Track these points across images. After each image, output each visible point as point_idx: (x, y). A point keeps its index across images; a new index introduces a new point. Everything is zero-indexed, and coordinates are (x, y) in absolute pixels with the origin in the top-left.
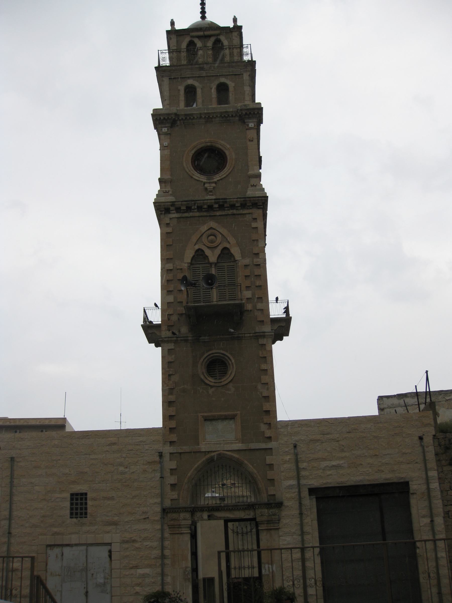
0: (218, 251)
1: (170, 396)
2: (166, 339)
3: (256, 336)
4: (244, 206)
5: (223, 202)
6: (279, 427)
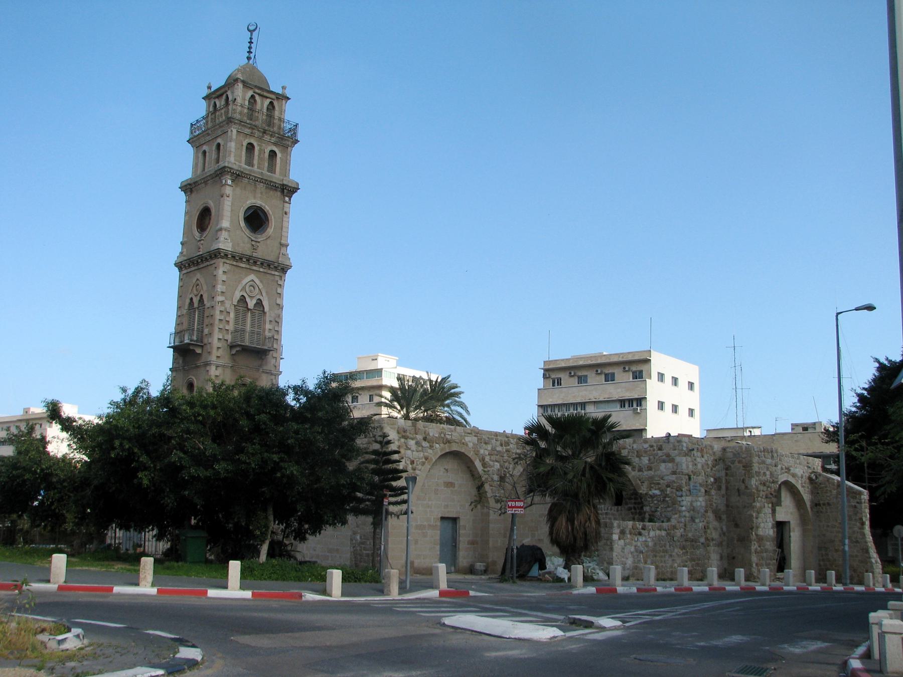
0: (254, 301)
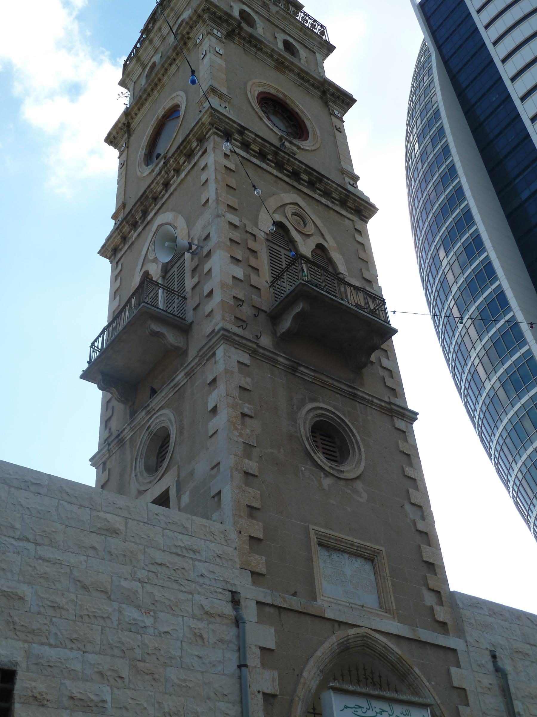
1: (246, 461)
2: (237, 338)
3: (391, 410)
4: (343, 203)
5: (317, 178)
6: (460, 605)
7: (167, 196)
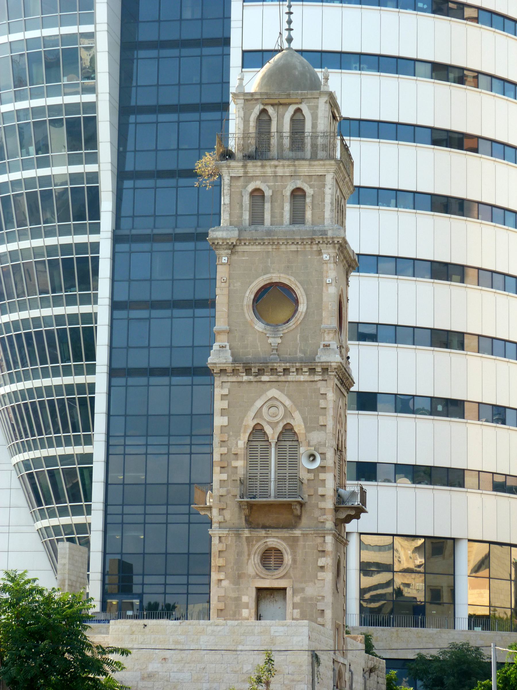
7: (283, 378)
